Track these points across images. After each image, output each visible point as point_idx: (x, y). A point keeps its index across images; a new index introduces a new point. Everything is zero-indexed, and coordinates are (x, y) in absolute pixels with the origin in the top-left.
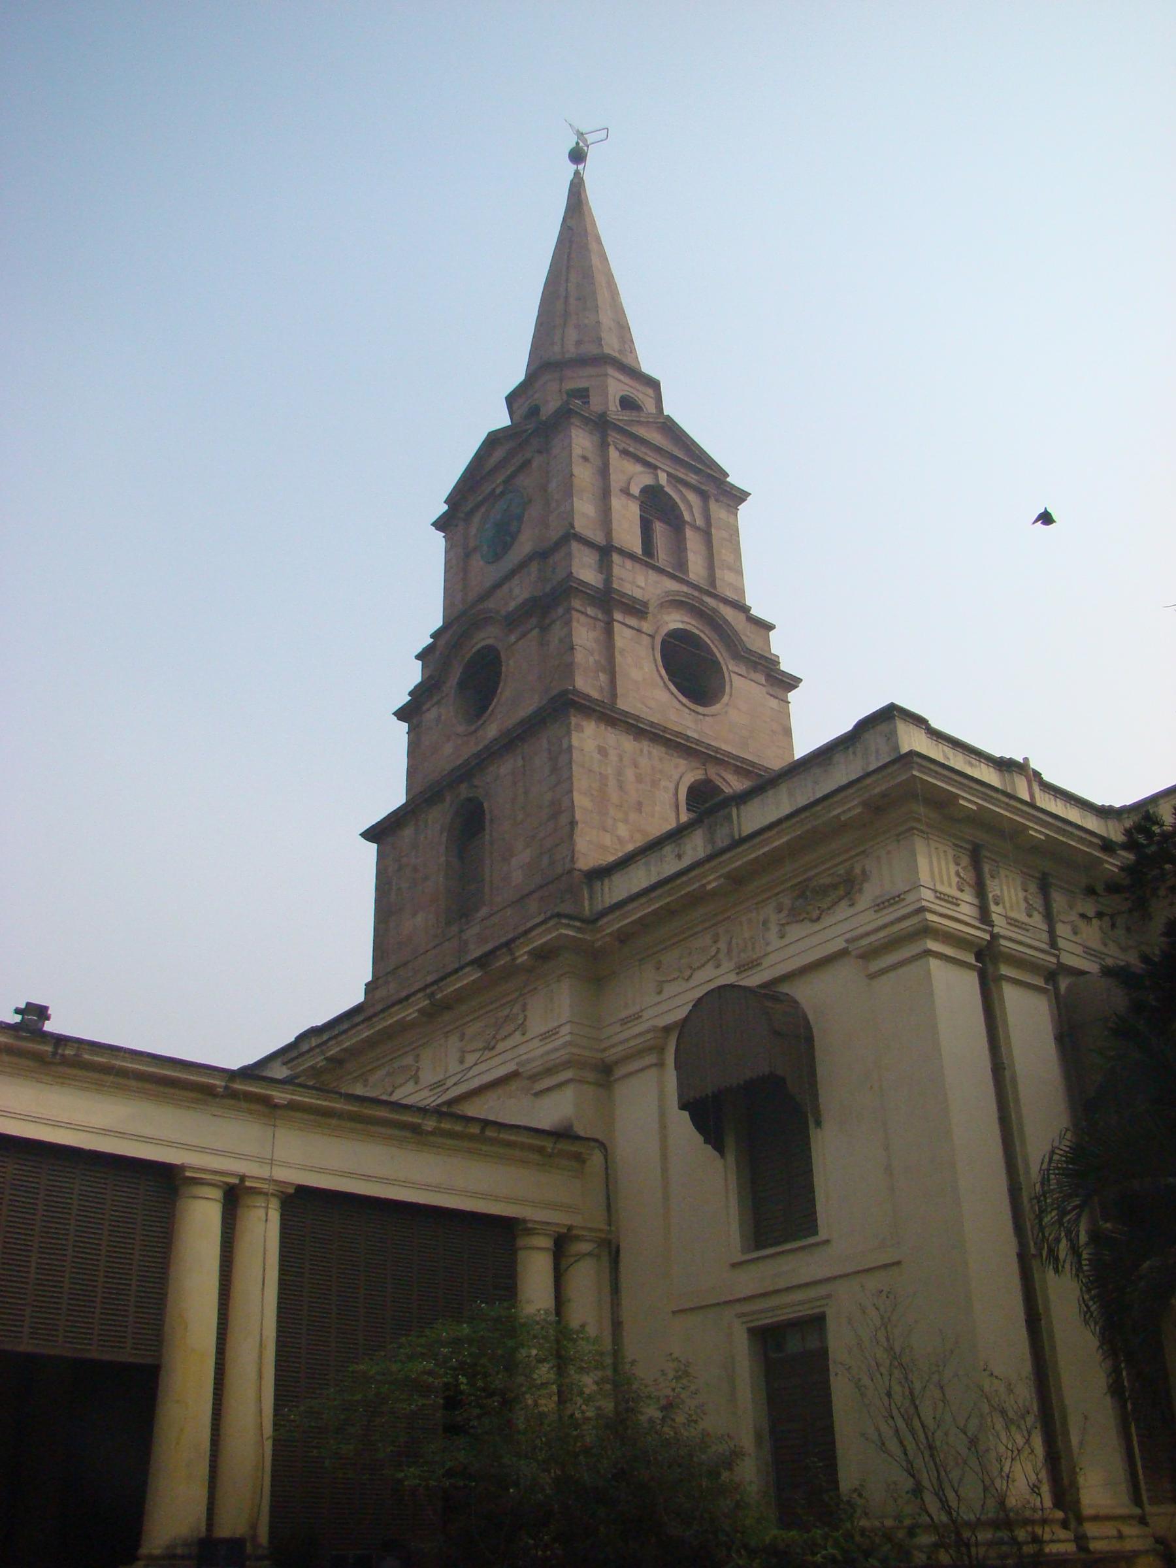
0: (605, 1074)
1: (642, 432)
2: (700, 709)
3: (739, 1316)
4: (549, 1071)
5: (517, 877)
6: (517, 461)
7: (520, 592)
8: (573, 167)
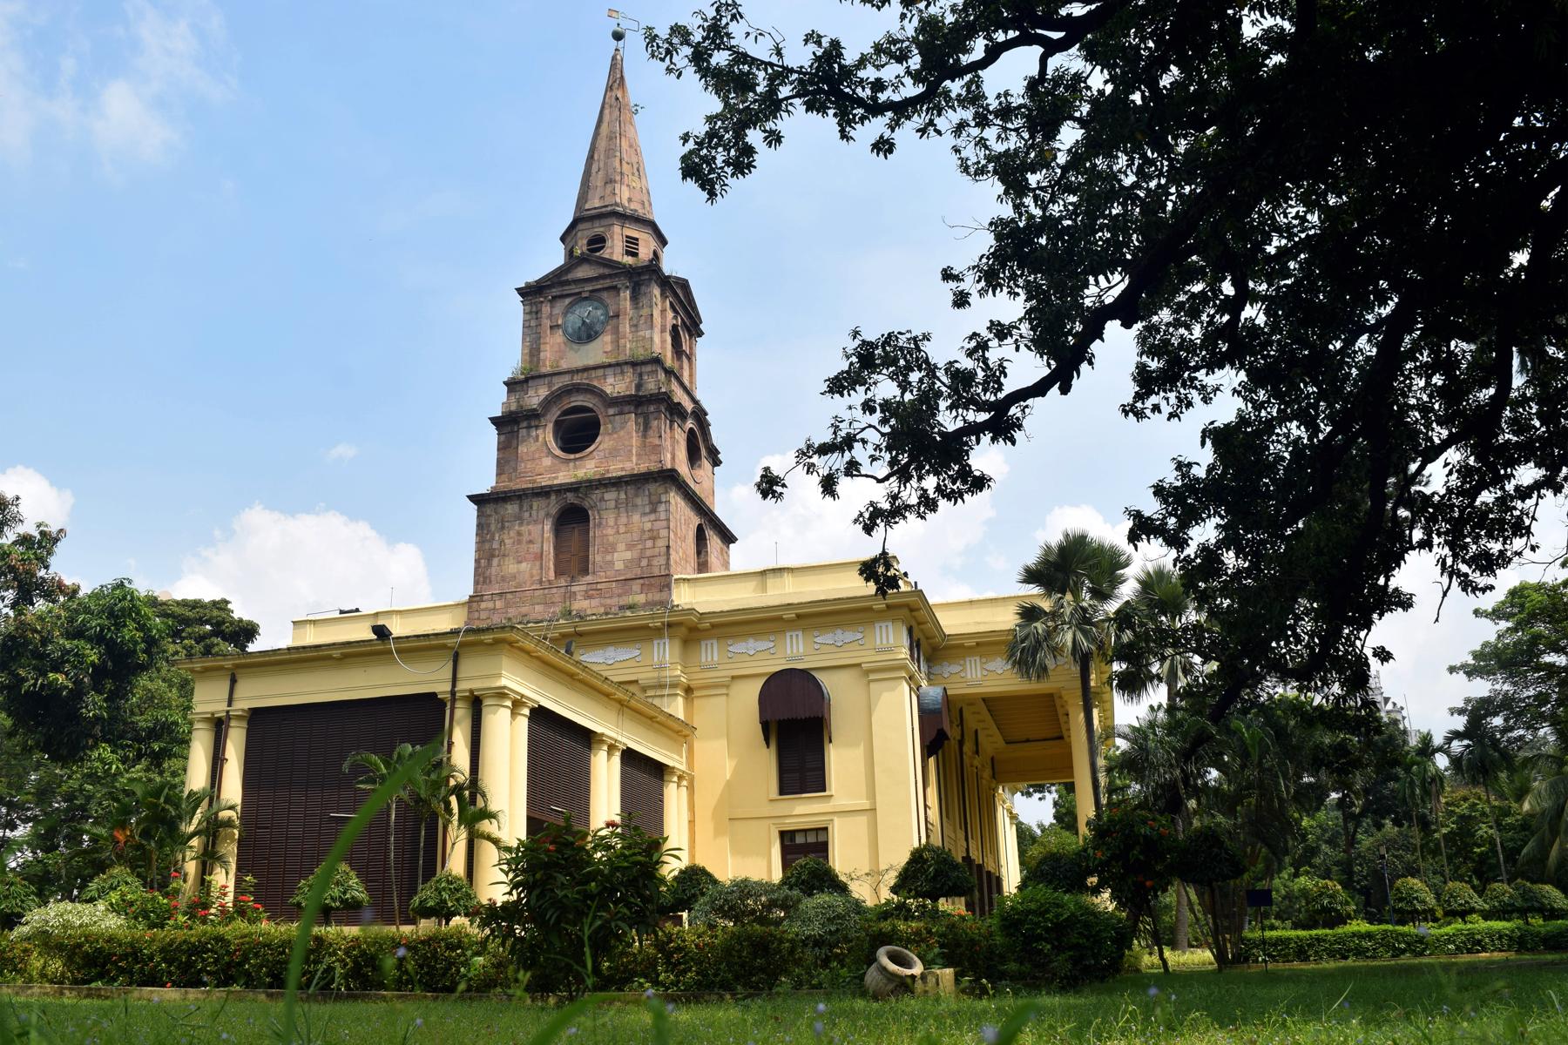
5: (619, 565)
6: (607, 283)
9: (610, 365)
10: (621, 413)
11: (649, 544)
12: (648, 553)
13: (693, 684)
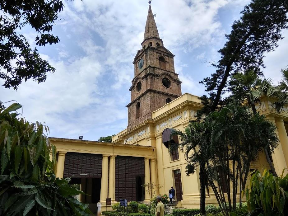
0: (154, 138)
1: (160, 49)
2: (168, 88)
4: (148, 138)
5: (144, 113)
7: (144, 74)
8: (149, 4)
13: (155, 136)
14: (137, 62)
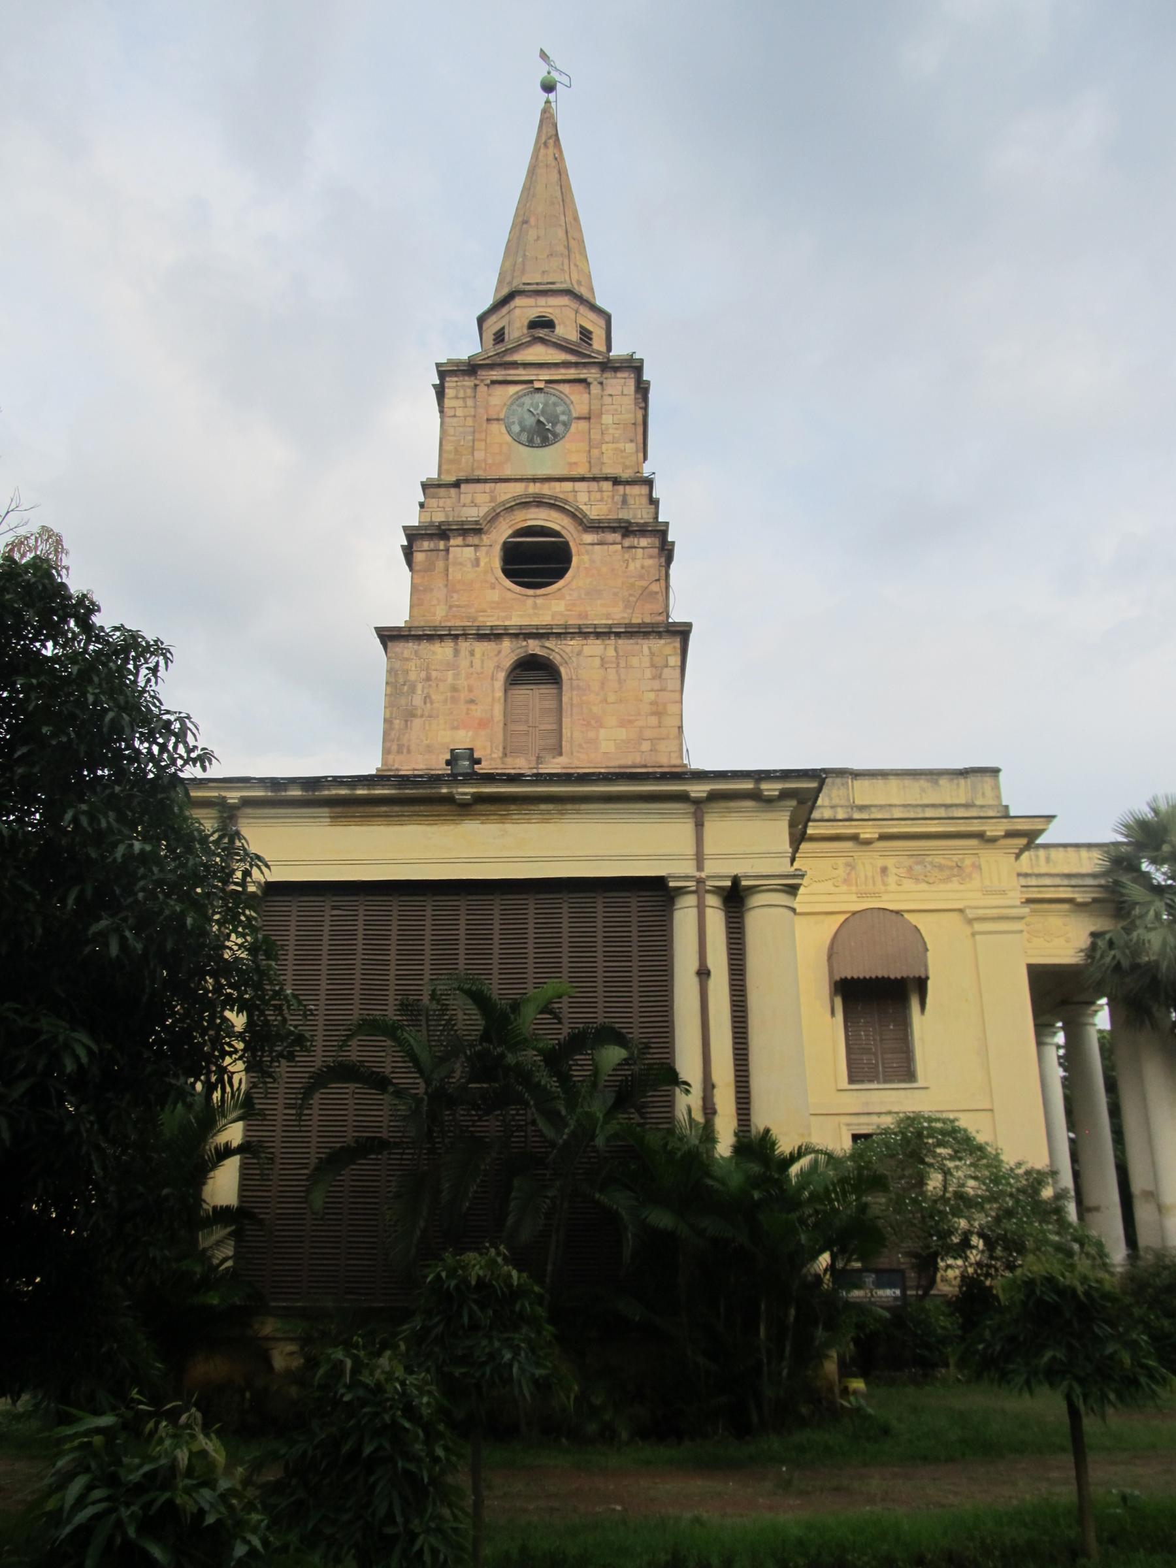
3: (848, 1125)
6: (572, 373)
9: (583, 479)
10: (600, 543)
11: (653, 720)
12: (648, 733)
14: (494, 382)
